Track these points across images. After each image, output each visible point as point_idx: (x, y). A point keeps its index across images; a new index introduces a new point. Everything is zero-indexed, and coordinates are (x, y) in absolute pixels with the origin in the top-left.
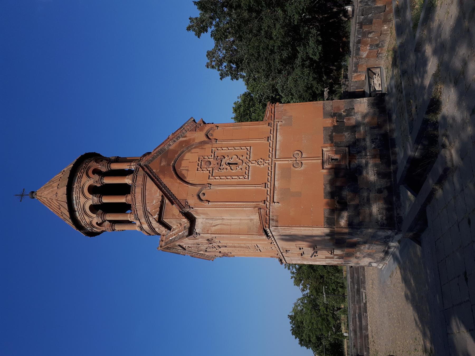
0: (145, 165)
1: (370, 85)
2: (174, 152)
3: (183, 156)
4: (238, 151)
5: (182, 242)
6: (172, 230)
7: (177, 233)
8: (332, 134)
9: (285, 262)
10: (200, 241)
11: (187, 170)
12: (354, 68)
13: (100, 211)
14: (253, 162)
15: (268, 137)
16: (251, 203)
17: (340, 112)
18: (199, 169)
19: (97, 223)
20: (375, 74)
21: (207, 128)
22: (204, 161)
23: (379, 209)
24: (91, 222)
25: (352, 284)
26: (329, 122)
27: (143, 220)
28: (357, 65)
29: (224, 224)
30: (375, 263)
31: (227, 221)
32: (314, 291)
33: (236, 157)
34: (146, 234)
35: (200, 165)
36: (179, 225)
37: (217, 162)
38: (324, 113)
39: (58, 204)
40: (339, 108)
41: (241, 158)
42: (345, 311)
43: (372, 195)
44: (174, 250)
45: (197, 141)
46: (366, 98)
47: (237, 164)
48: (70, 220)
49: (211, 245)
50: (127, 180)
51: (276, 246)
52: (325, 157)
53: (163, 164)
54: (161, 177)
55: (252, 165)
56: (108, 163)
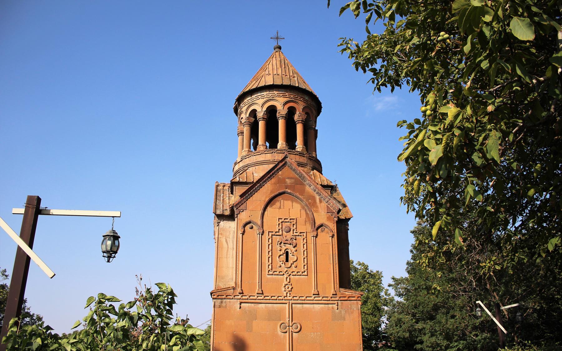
2: (302, 192)
3: (297, 202)
4: (301, 263)
6: (231, 195)
11: (280, 208)
13: (252, 119)
14: (288, 279)
15: (318, 294)
18: (281, 221)
27: (241, 164)
31: (231, 254)
35: (286, 220)
47: (287, 260)
50: (281, 143)
53: (288, 181)
54: (273, 180)
56: (302, 121)
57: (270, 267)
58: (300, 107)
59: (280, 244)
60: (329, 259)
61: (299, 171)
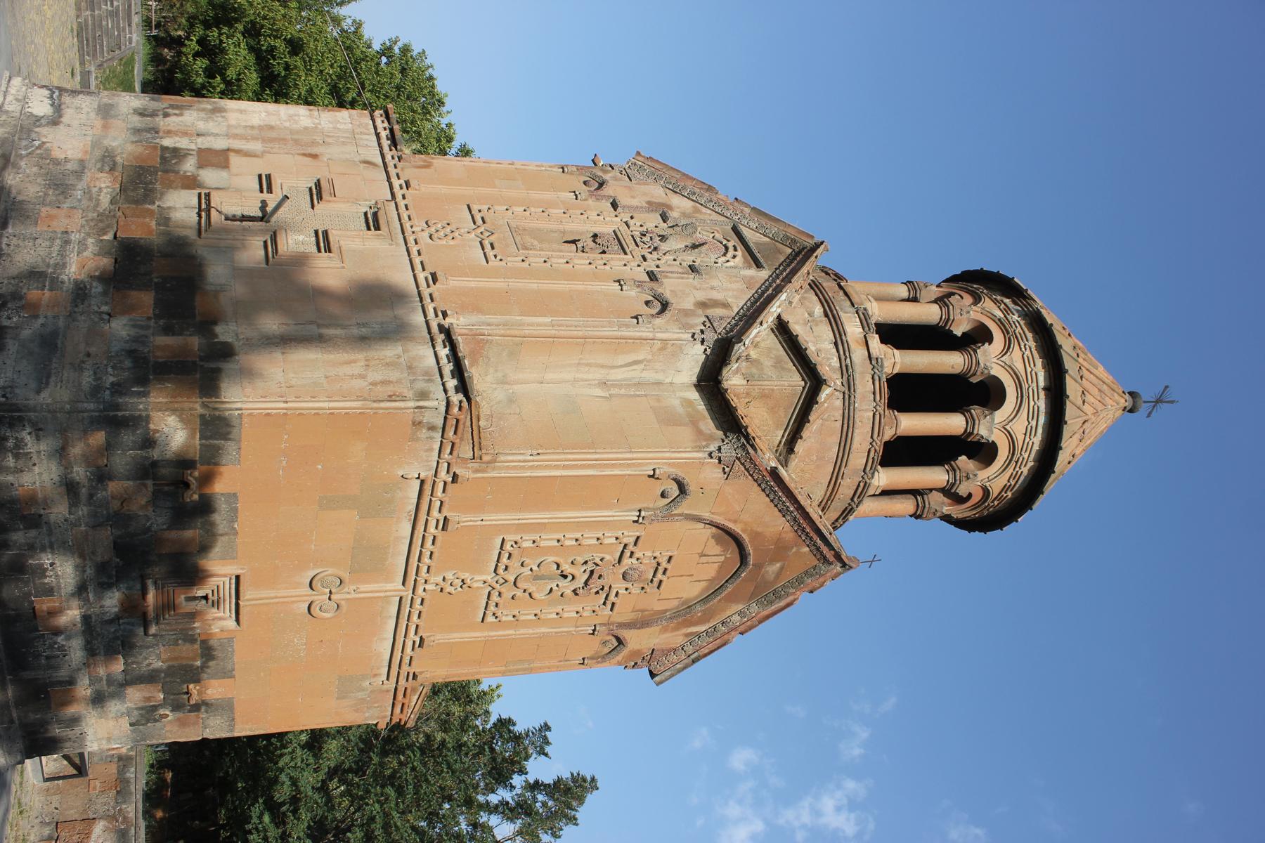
0: (830, 564)
2: (731, 599)
3: (707, 589)
5: (749, 282)
11: (702, 555)
17: (179, 715)
26: (214, 689)
27: (858, 354)
29: (602, 366)
31: (590, 376)
33: (534, 595)
36: (753, 354)
41: (519, 593)
45: (655, 629)
52: (229, 605)
55: (484, 577)
57: (529, 544)
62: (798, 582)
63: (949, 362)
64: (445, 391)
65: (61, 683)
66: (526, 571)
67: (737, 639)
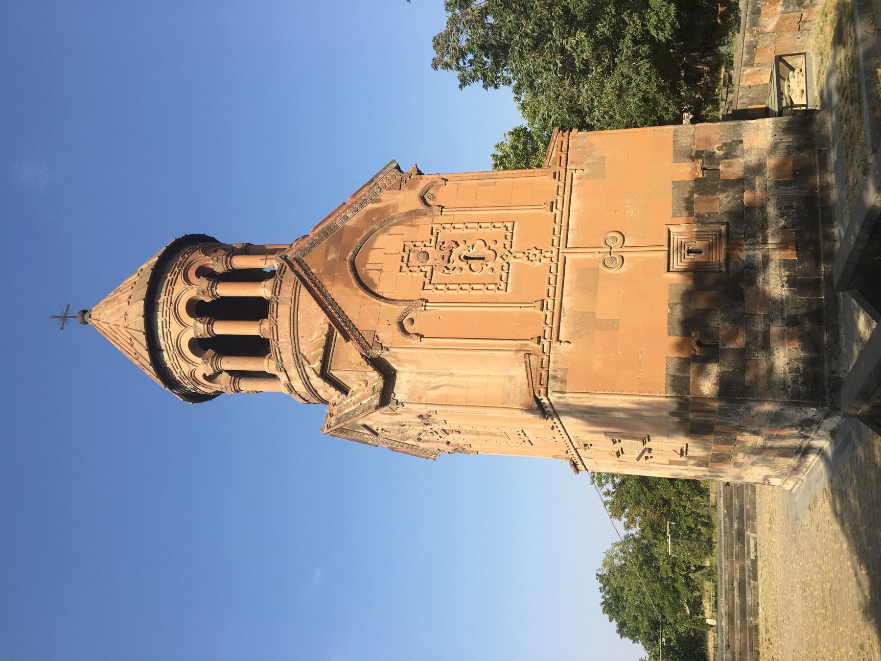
0: (295, 259)
1: (780, 94)
2: (356, 231)
3: (373, 242)
4: (487, 232)
6: (350, 393)
7: (359, 401)
8: (692, 196)
9: (583, 468)
10: (404, 418)
11: (380, 270)
12: (746, 57)
13: (210, 352)
14: (518, 255)
15: (552, 203)
16: (511, 342)
17: (710, 149)
18: (405, 269)
19: (204, 376)
20: (793, 69)
21: (423, 183)
22: (414, 251)
23: (790, 359)
24: (192, 373)
25: (727, 519)
26: (687, 171)
27: (293, 372)
28: (752, 49)
29: (454, 386)
30: (777, 477)
32: (648, 529)
33: (482, 243)
34: (302, 401)
35: (405, 259)
36: (363, 385)
37: (442, 253)
38: (675, 151)
39: (129, 336)
40: (708, 141)
41: (493, 246)
42: (711, 574)
43: (775, 329)
44: (354, 436)
45: (402, 210)
46: (771, 119)
47: (483, 259)
48: (151, 368)
49: (428, 428)
50: (262, 290)
51: (564, 435)
54: (326, 283)
55: (516, 260)
56: (227, 256)
57: (490, 287)
58: (200, 259)
59: (448, 269)
60: (485, 185)
61: (315, 235)
62: (313, 245)
63: (230, 364)
64: (548, 399)
65: (786, 184)
66: (490, 264)
67: (348, 200)
